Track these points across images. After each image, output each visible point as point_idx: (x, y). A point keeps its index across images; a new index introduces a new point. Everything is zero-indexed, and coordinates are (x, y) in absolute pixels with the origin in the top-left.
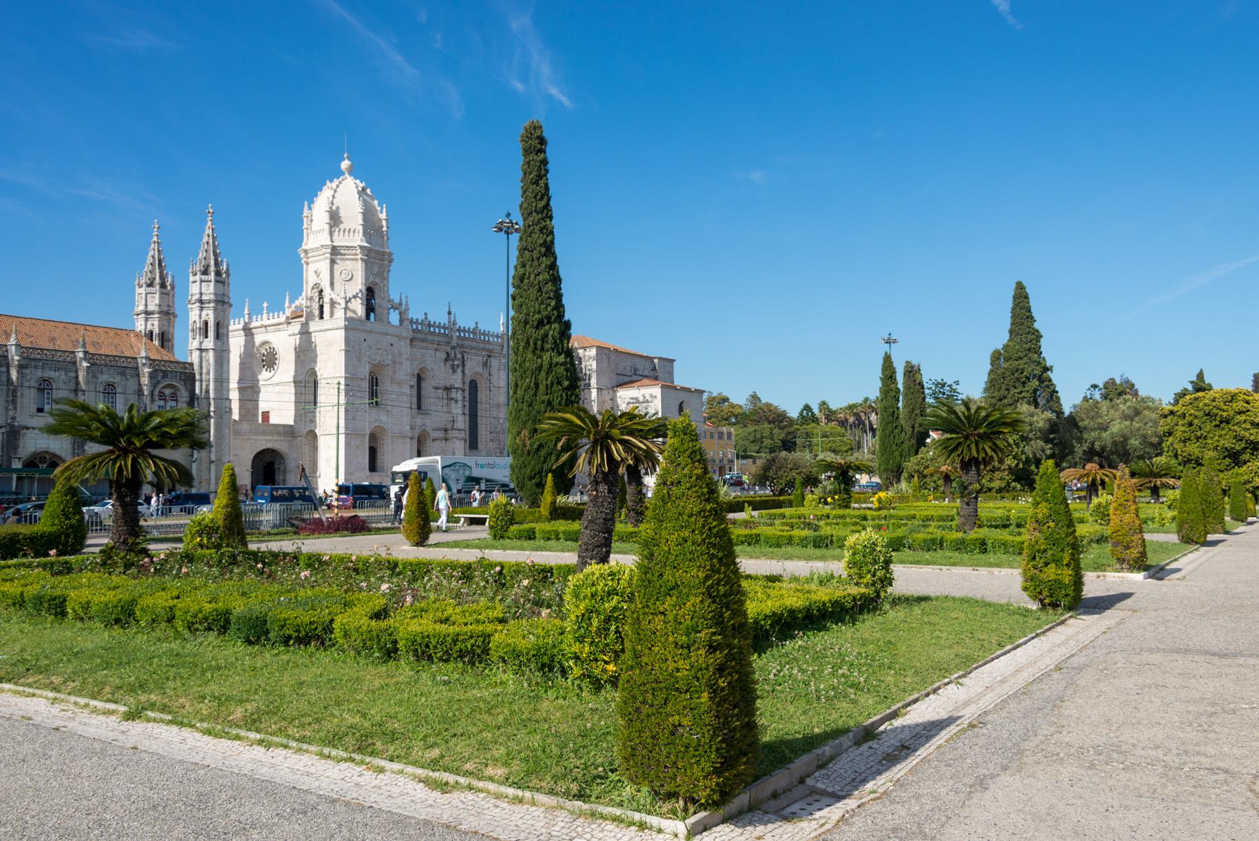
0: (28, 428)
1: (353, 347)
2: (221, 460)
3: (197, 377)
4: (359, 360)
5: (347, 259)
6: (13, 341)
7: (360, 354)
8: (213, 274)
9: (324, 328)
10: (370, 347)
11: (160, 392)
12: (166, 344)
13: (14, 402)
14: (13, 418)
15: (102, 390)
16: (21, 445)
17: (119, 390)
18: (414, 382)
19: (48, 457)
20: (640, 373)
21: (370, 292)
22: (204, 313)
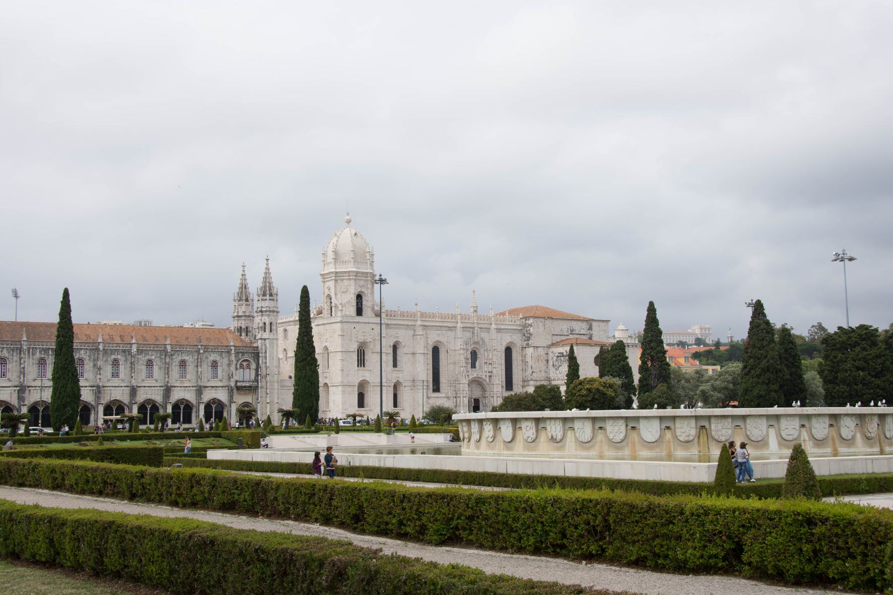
0: (175, 387)
1: (347, 333)
2: (273, 402)
3: (260, 355)
4: (351, 340)
5: (343, 280)
6: (168, 342)
7: (351, 336)
8: (268, 295)
9: (331, 322)
10: (358, 332)
11: (241, 364)
12: (249, 334)
13: (168, 374)
14: (168, 382)
15: (210, 365)
16: (171, 396)
17: (219, 364)
18: (391, 351)
19: (184, 401)
20: (577, 332)
21: (359, 297)
22: (263, 318)
